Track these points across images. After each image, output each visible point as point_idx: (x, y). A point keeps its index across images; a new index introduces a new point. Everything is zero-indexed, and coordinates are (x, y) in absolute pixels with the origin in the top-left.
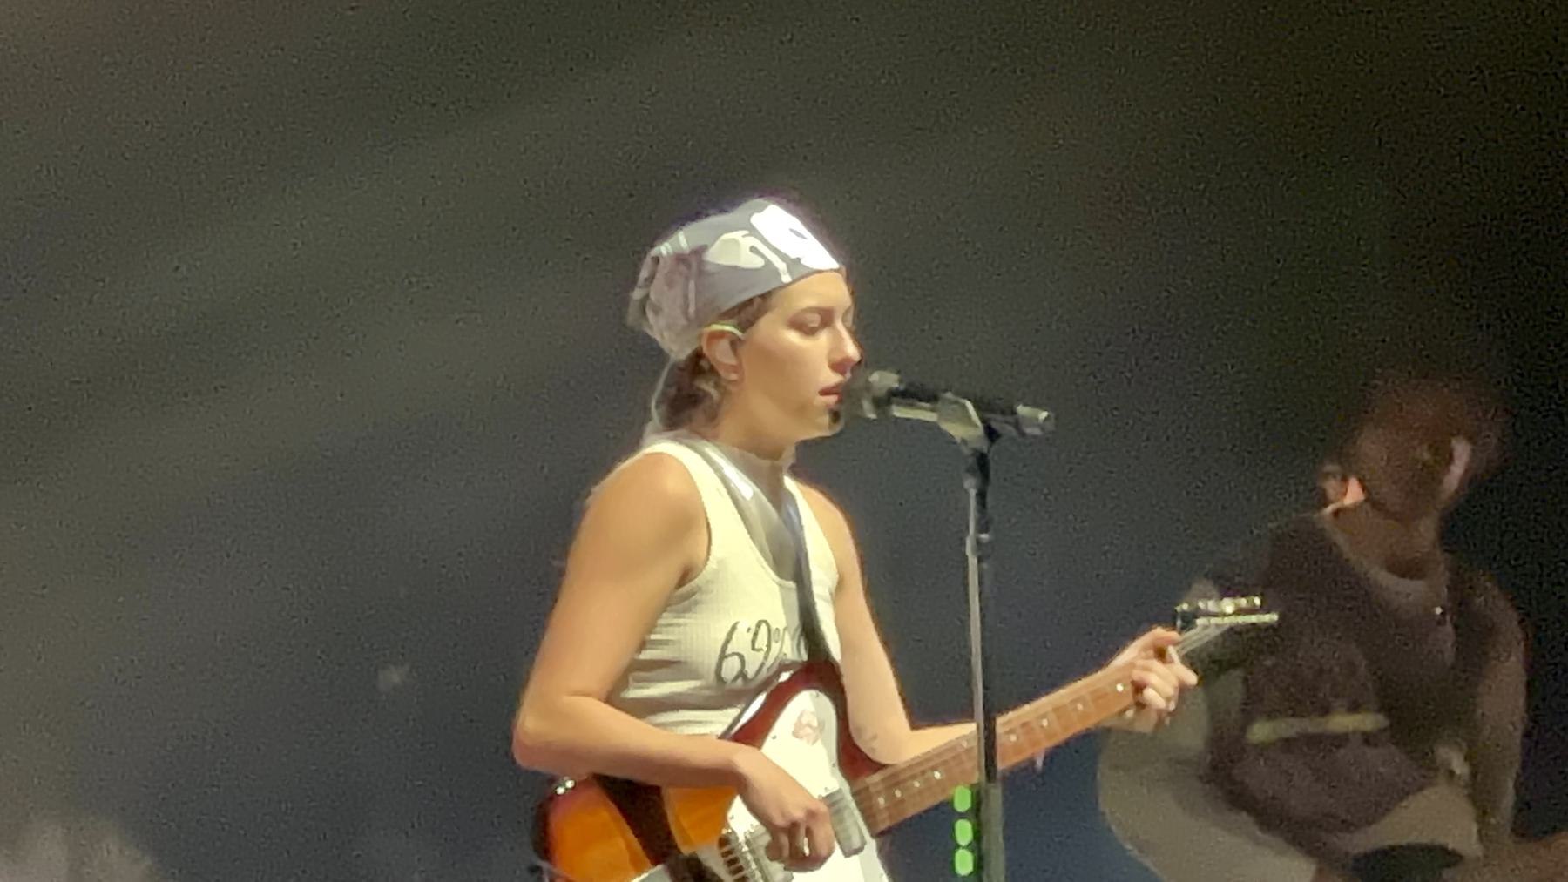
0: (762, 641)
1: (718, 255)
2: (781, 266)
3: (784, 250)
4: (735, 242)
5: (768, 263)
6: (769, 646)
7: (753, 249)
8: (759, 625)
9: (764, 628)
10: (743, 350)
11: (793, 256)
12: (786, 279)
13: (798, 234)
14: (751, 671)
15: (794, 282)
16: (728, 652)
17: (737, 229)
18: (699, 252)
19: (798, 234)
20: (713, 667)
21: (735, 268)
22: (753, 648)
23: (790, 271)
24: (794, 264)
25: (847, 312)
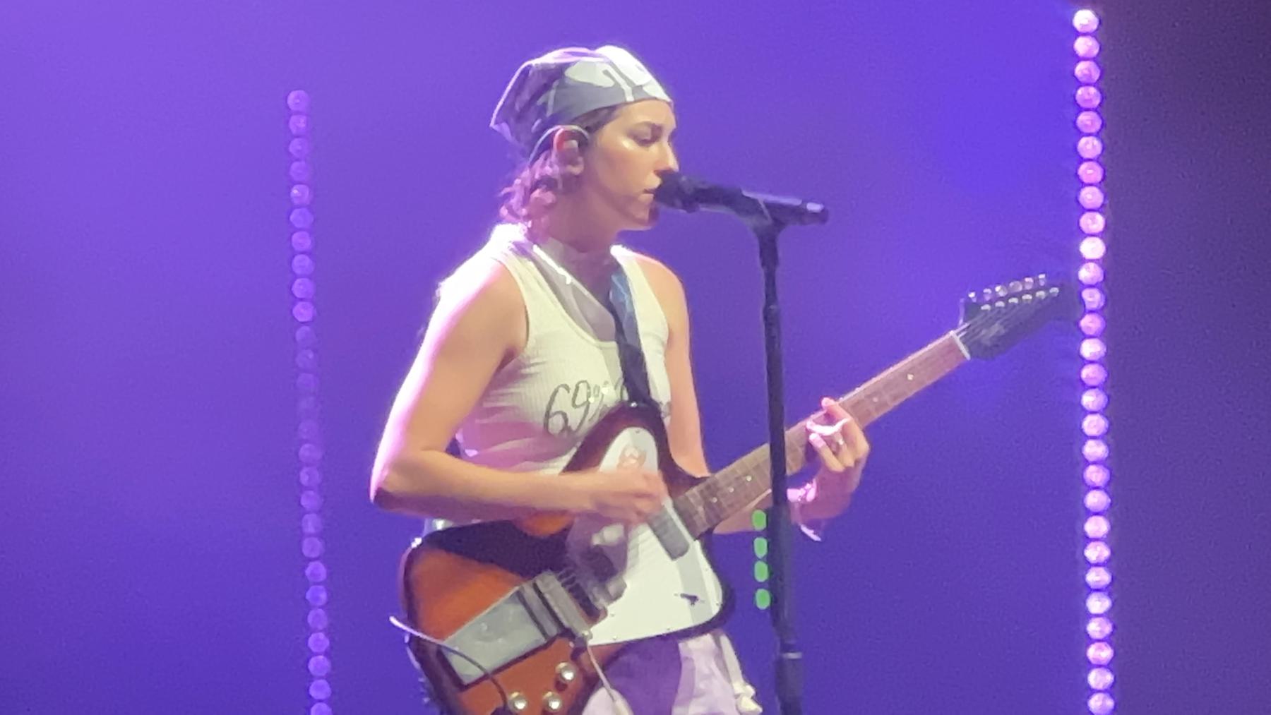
0: (581, 398)
3: (631, 77)
5: (617, 88)
6: (587, 404)
7: (606, 73)
11: (638, 83)
14: (574, 422)
15: (636, 101)
16: (554, 409)
18: (558, 72)
20: (540, 419)
22: (574, 405)
24: (637, 89)
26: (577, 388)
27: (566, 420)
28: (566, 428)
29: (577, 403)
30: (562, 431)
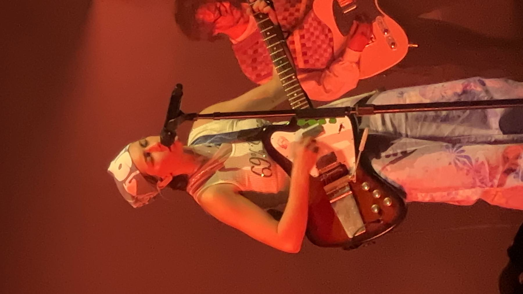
0: (257, 161)
1: (134, 193)
2: (133, 174)
4: (128, 188)
5: (134, 177)
6: (259, 159)
8: (252, 163)
9: (252, 160)
11: (129, 170)
12: (138, 172)
14: (267, 165)
15: (138, 170)
17: (124, 187)
22: (259, 165)
26: (252, 163)
27: (266, 168)
28: (268, 168)
30: (270, 170)
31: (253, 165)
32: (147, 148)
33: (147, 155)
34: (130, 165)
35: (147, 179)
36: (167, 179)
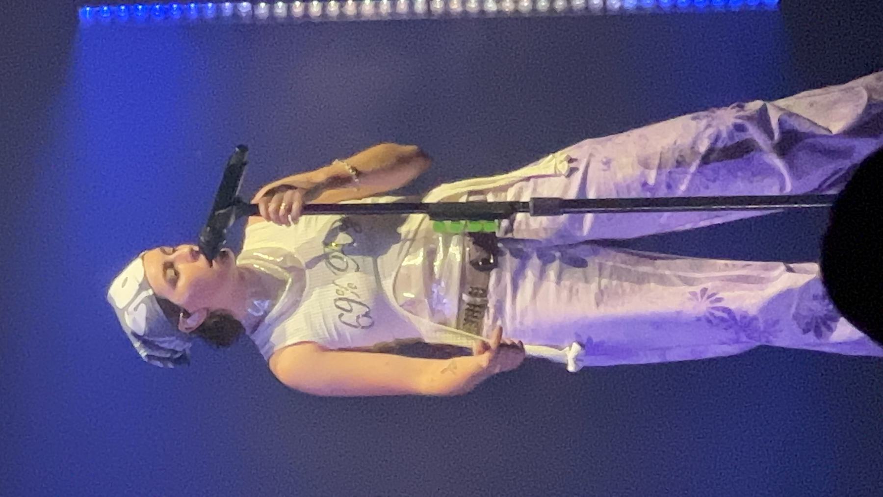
1: (141, 327)
2: (144, 294)
8: (338, 307)
9: (339, 303)
10: (190, 311)
11: (137, 287)
13: (126, 280)
15: (151, 287)
16: (356, 324)
19: (126, 280)
21: (147, 318)
23: (147, 289)
25: (164, 252)
26: (338, 307)
29: (349, 308)
31: (340, 311)
32: (171, 258)
33: (169, 265)
34: (140, 279)
35: (168, 310)
36: (197, 315)
